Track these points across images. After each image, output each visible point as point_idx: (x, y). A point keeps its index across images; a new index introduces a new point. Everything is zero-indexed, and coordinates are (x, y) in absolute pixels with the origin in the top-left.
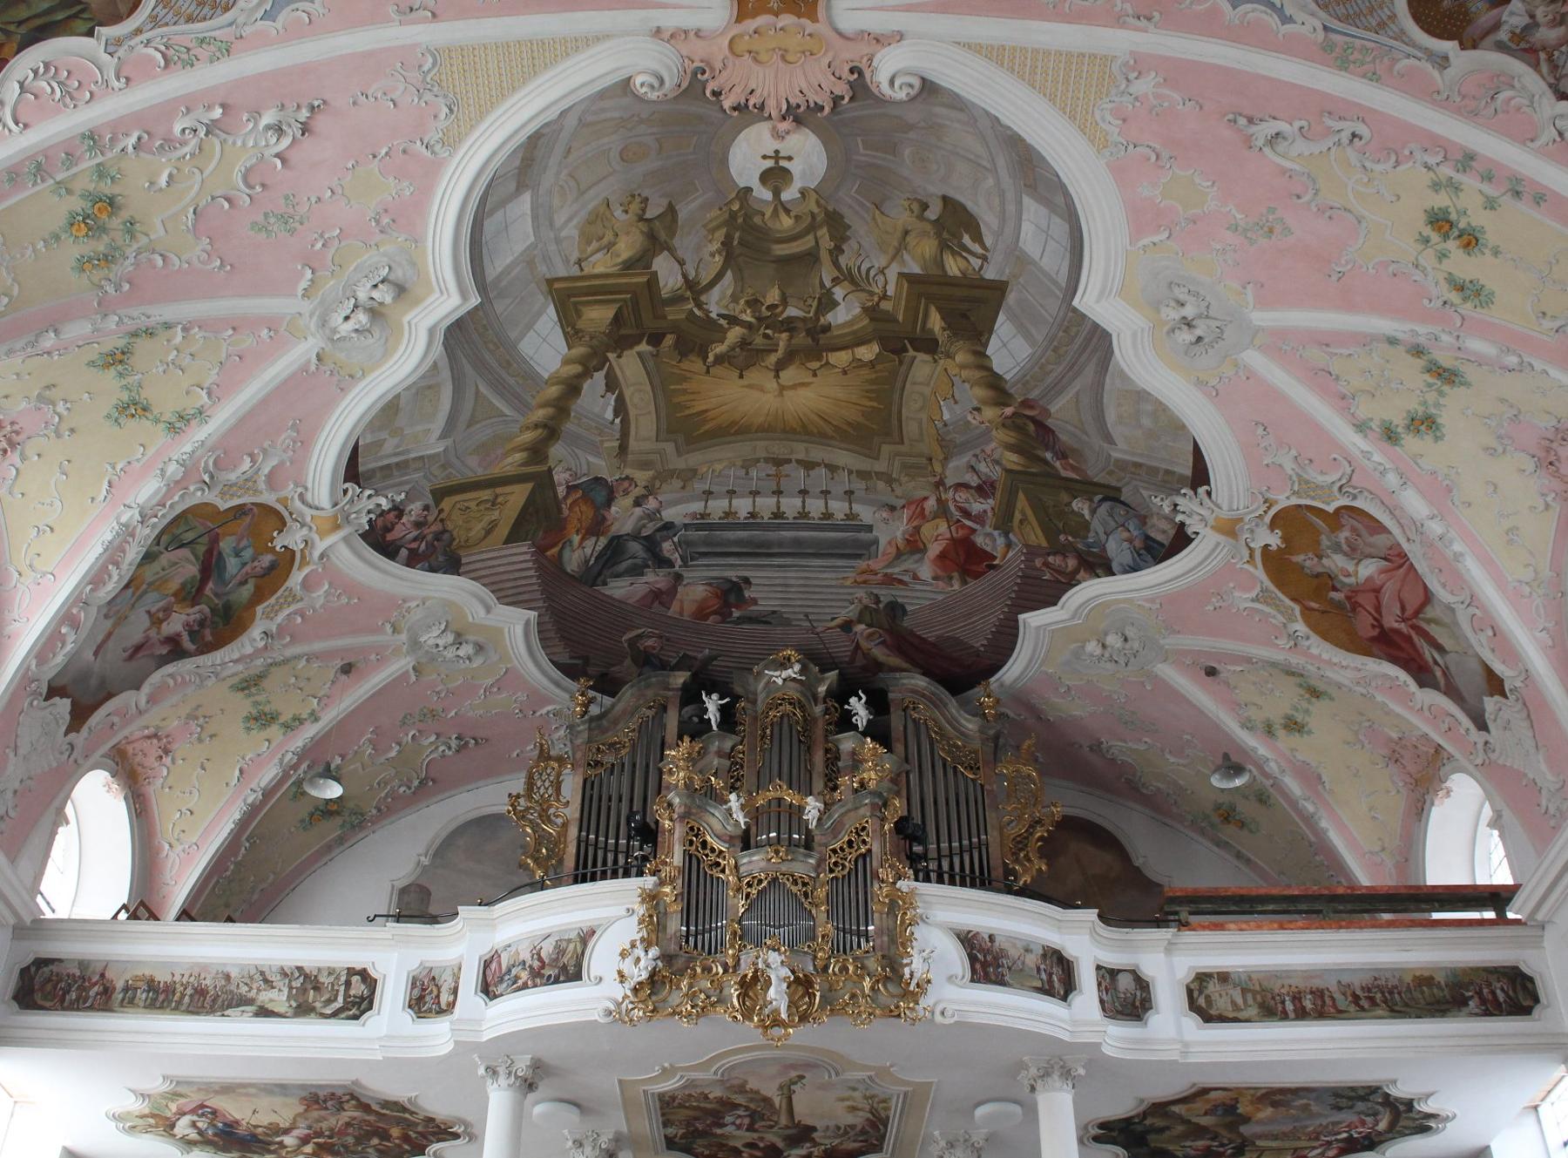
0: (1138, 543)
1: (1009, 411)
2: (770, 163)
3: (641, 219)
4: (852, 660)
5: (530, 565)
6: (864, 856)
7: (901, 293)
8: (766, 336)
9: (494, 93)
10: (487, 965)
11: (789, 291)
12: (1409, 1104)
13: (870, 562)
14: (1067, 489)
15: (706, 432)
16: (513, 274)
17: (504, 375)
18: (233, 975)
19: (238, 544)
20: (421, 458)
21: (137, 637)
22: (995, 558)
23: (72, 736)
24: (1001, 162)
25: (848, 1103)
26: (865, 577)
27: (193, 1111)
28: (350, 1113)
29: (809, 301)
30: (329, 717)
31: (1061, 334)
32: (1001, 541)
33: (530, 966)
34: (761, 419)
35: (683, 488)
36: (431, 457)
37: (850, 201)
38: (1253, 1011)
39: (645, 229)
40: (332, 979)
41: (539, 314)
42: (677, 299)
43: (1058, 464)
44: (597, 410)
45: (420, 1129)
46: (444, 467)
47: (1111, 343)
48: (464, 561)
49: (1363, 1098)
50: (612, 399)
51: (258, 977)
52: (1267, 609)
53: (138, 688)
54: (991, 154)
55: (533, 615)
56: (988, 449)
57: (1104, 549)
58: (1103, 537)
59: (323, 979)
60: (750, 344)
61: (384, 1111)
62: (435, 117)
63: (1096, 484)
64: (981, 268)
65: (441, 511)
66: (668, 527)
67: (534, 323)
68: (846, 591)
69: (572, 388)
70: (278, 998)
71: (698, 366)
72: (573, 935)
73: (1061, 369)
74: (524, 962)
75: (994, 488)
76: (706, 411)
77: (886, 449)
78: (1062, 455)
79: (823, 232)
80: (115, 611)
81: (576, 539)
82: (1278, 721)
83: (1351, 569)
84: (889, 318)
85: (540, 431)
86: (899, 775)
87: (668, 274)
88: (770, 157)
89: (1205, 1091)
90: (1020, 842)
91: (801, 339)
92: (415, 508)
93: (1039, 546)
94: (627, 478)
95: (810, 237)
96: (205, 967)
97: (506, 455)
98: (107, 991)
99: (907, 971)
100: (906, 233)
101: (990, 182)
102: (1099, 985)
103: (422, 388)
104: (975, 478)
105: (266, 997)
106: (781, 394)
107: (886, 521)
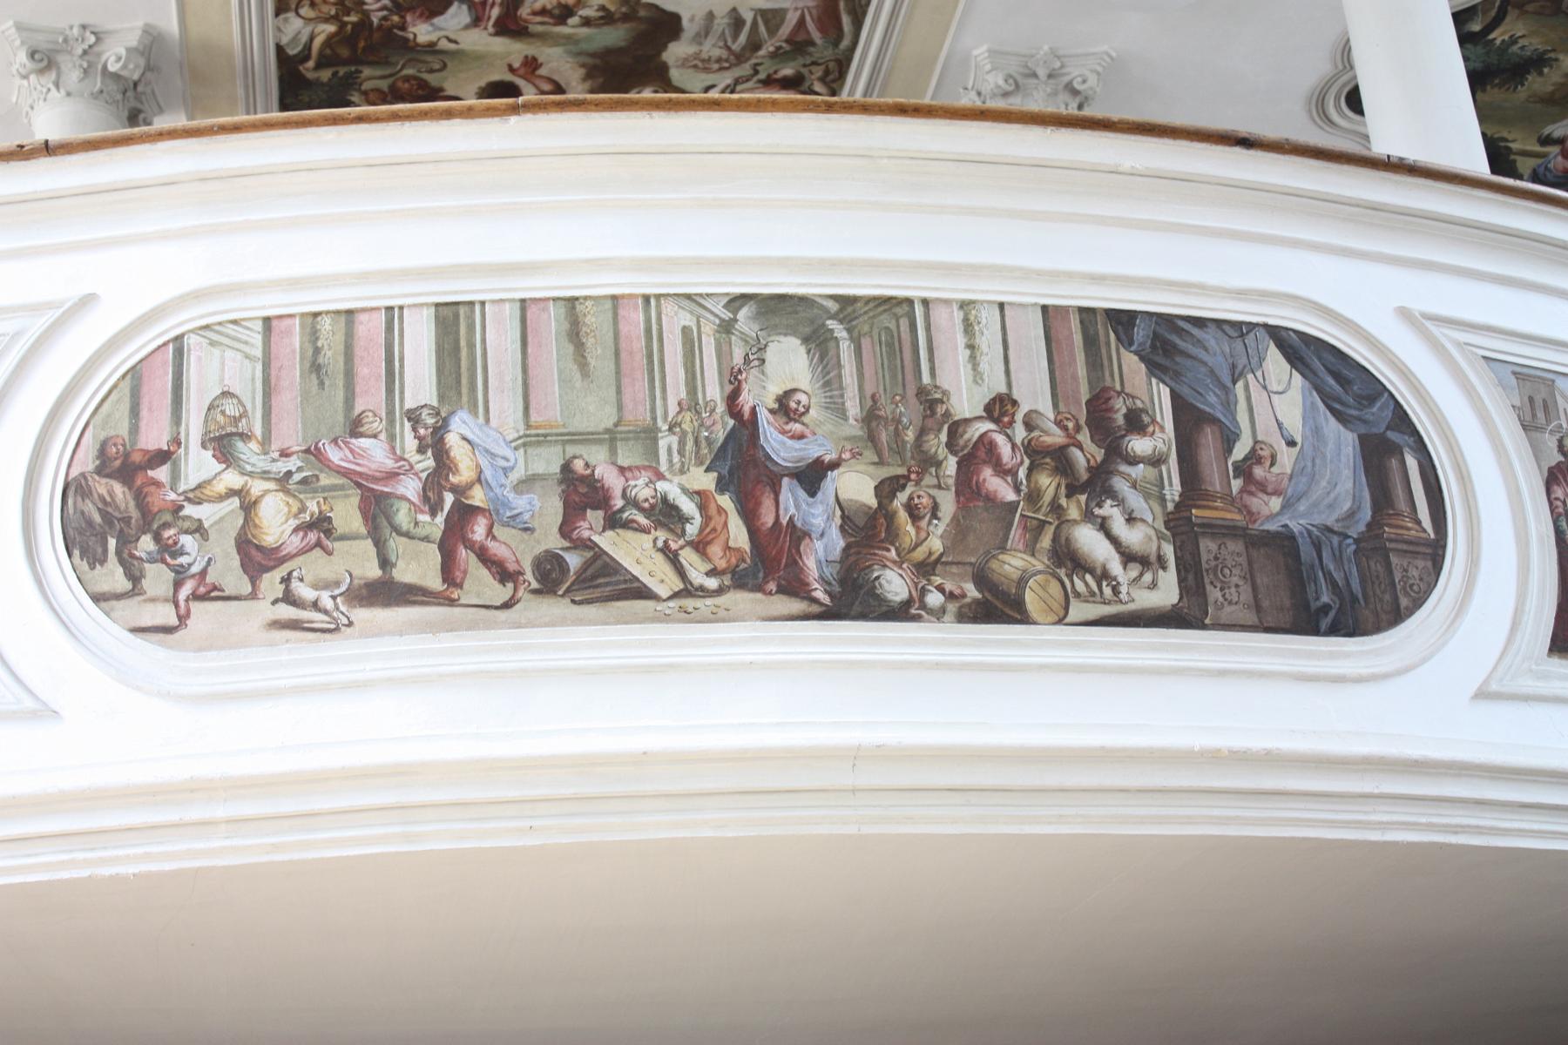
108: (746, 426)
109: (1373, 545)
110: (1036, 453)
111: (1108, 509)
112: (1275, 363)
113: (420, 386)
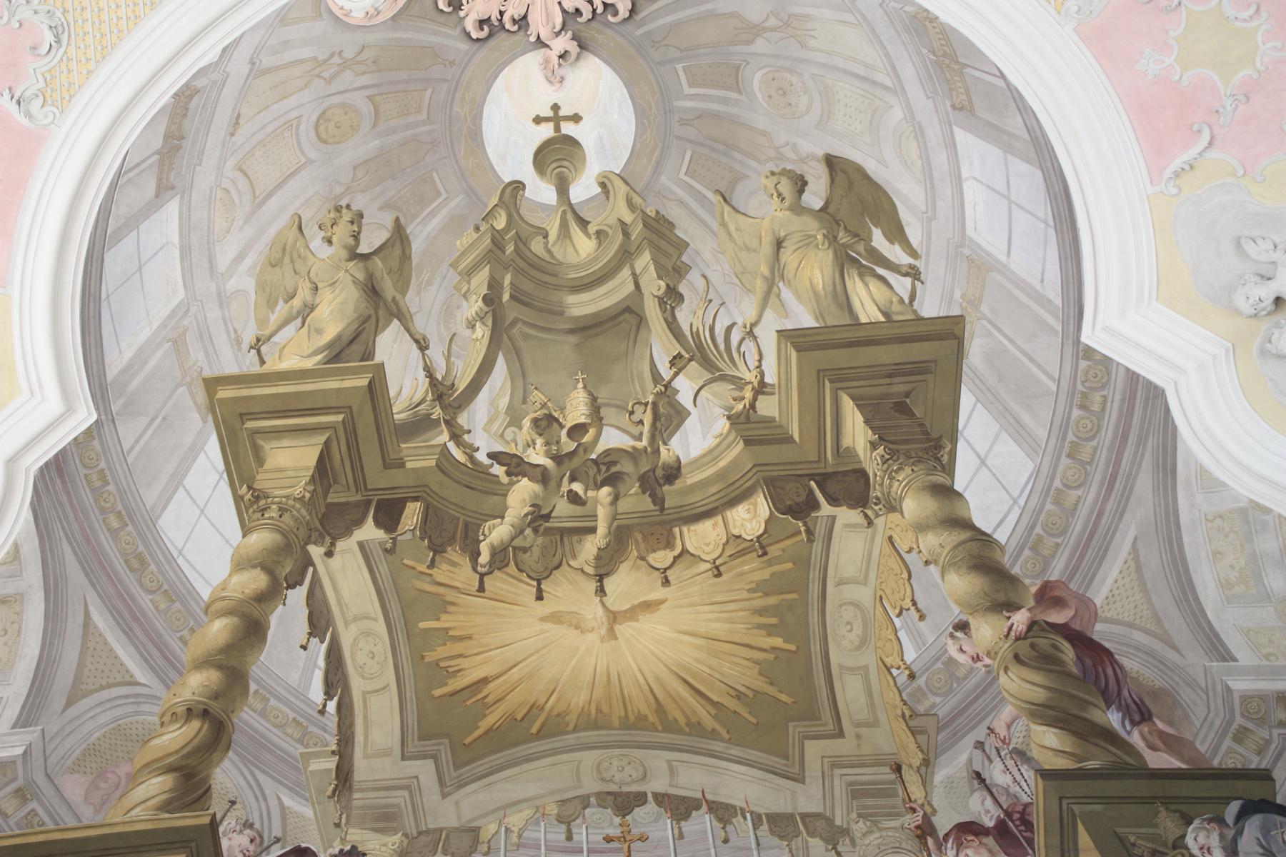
2: (547, 131)
3: (354, 255)
7: (788, 380)
8: (574, 498)
9: (122, 12)
11: (603, 395)
14: (1167, 801)
16: (151, 364)
17: (130, 581)
24: (908, 72)
29: (639, 409)
31: (1076, 413)
34: (579, 699)
37: (681, 193)
39: (361, 276)
41: (195, 450)
42: (419, 425)
43: (1136, 738)
44: (294, 678)
46: (22, 795)
47: (1167, 411)
50: (320, 650)
54: (887, 55)
60: (547, 517)
62: (34, 48)
64: (913, 297)
71: (464, 575)
73: (1091, 497)
75: (1029, 826)
76: (484, 681)
77: (813, 749)
78: (1140, 714)
79: (644, 261)
85: (196, 724)
88: (547, 120)
91: (635, 501)
95: (626, 272)
97: (134, 779)
100: (779, 244)
101: (897, 113)
104: (989, 802)
106: (612, 634)
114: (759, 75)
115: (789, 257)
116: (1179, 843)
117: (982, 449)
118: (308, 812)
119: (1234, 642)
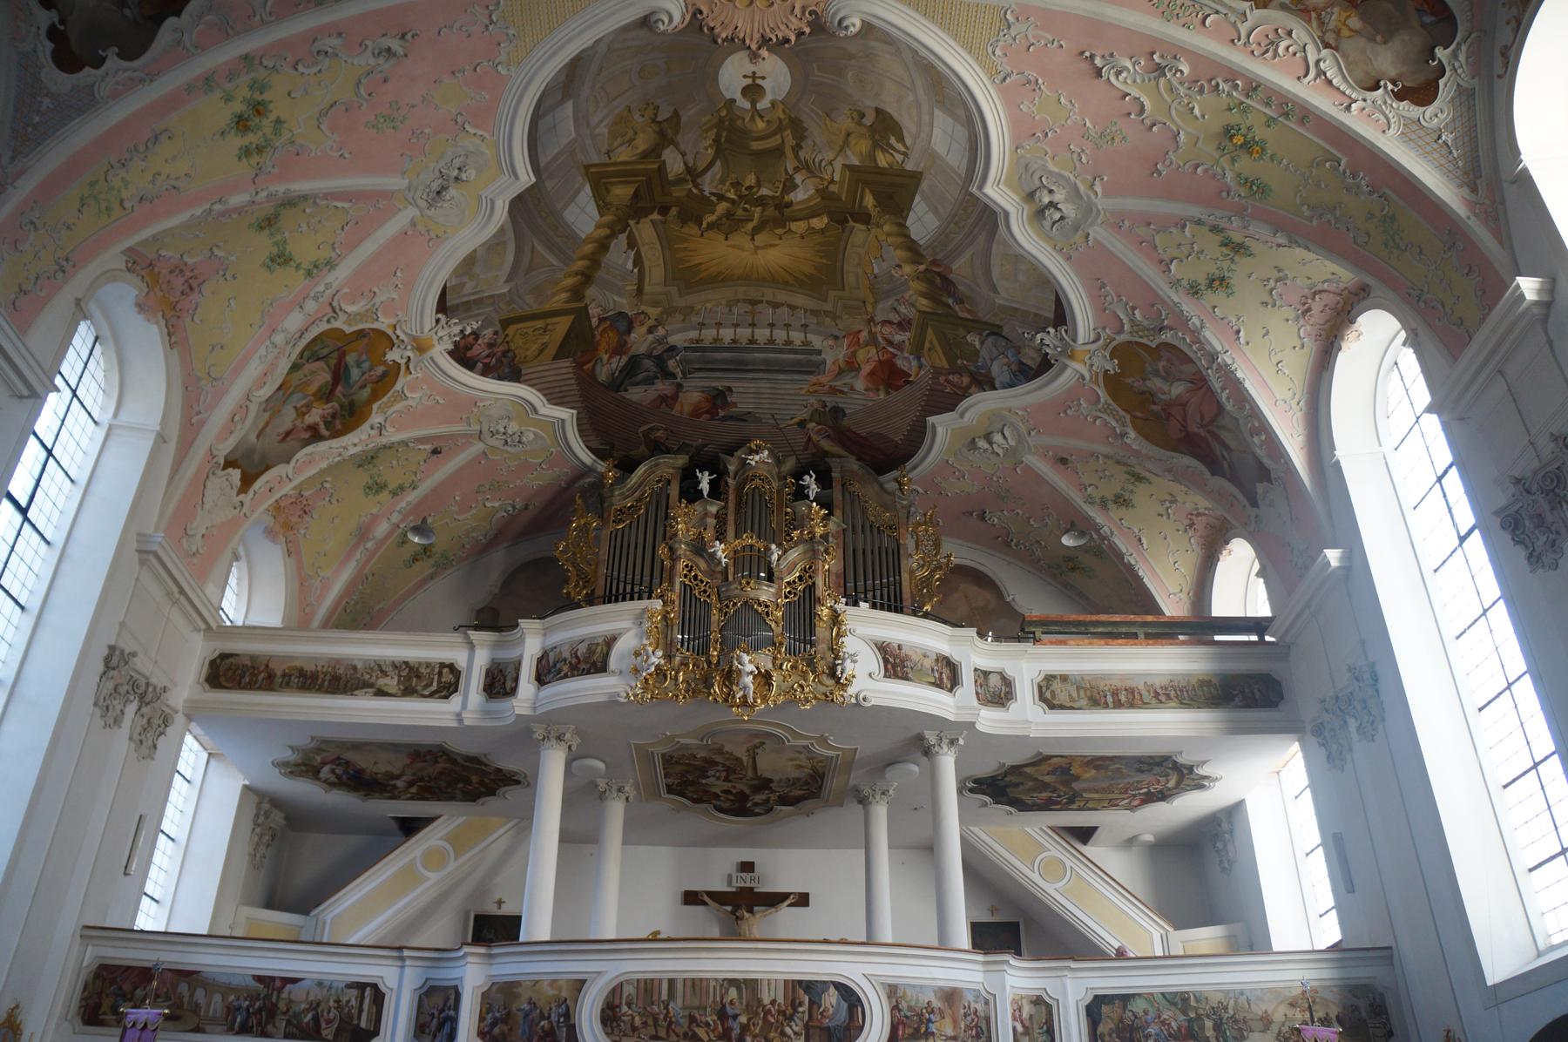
0: (1014, 367)
1: (922, 267)
2: (749, 81)
3: (654, 121)
4: (806, 449)
5: (571, 376)
6: (810, 587)
7: (844, 180)
8: (745, 209)
10: (540, 660)
12: (1191, 769)
13: (820, 377)
15: (701, 279)
18: (359, 667)
19: (360, 356)
20: (493, 296)
21: (288, 426)
22: (910, 376)
23: (242, 497)
24: (919, 83)
25: (798, 763)
26: (816, 388)
27: (332, 762)
28: (442, 765)
30: (425, 487)
31: (961, 212)
32: (915, 363)
33: (570, 663)
35: (684, 320)
36: (499, 295)
38: (1084, 702)
39: (657, 129)
40: (428, 670)
41: (578, 192)
42: (679, 181)
43: (957, 308)
45: (492, 777)
48: (523, 372)
49: (1159, 764)
51: (376, 668)
52: (1105, 416)
53: (288, 462)
55: (575, 412)
56: (907, 296)
57: (990, 372)
58: (989, 362)
59: (423, 670)
61: (467, 764)
63: (985, 323)
65: (507, 335)
66: (672, 349)
67: (575, 198)
68: (801, 398)
69: (603, 246)
70: (391, 683)
71: (695, 230)
72: (600, 640)
74: (565, 660)
76: (700, 264)
77: (832, 294)
78: (960, 301)
80: (271, 407)
81: (606, 357)
82: (1109, 495)
83: (1166, 388)
84: (834, 197)
85: (579, 277)
86: (837, 532)
87: (674, 163)
89: (1050, 757)
90: (923, 582)
92: (488, 333)
93: (943, 368)
94: (643, 312)
95: (778, 136)
96: (338, 661)
97: (554, 295)
98: (271, 677)
99: (839, 668)
100: (848, 135)
101: (911, 98)
102: (976, 681)
103: (495, 245)
105: (382, 682)
106: (756, 253)
107: (831, 347)
108: (724, 1007)
109: (848, 1028)
110: (779, 1012)
111: (793, 1024)
112: (832, 989)
113: (664, 996)
114: (850, 73)
115: (852, 140)
116: (964, 337)
117: (920, 214)
118: (624, 301)
119: (1000, 290)
